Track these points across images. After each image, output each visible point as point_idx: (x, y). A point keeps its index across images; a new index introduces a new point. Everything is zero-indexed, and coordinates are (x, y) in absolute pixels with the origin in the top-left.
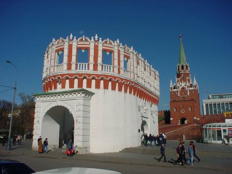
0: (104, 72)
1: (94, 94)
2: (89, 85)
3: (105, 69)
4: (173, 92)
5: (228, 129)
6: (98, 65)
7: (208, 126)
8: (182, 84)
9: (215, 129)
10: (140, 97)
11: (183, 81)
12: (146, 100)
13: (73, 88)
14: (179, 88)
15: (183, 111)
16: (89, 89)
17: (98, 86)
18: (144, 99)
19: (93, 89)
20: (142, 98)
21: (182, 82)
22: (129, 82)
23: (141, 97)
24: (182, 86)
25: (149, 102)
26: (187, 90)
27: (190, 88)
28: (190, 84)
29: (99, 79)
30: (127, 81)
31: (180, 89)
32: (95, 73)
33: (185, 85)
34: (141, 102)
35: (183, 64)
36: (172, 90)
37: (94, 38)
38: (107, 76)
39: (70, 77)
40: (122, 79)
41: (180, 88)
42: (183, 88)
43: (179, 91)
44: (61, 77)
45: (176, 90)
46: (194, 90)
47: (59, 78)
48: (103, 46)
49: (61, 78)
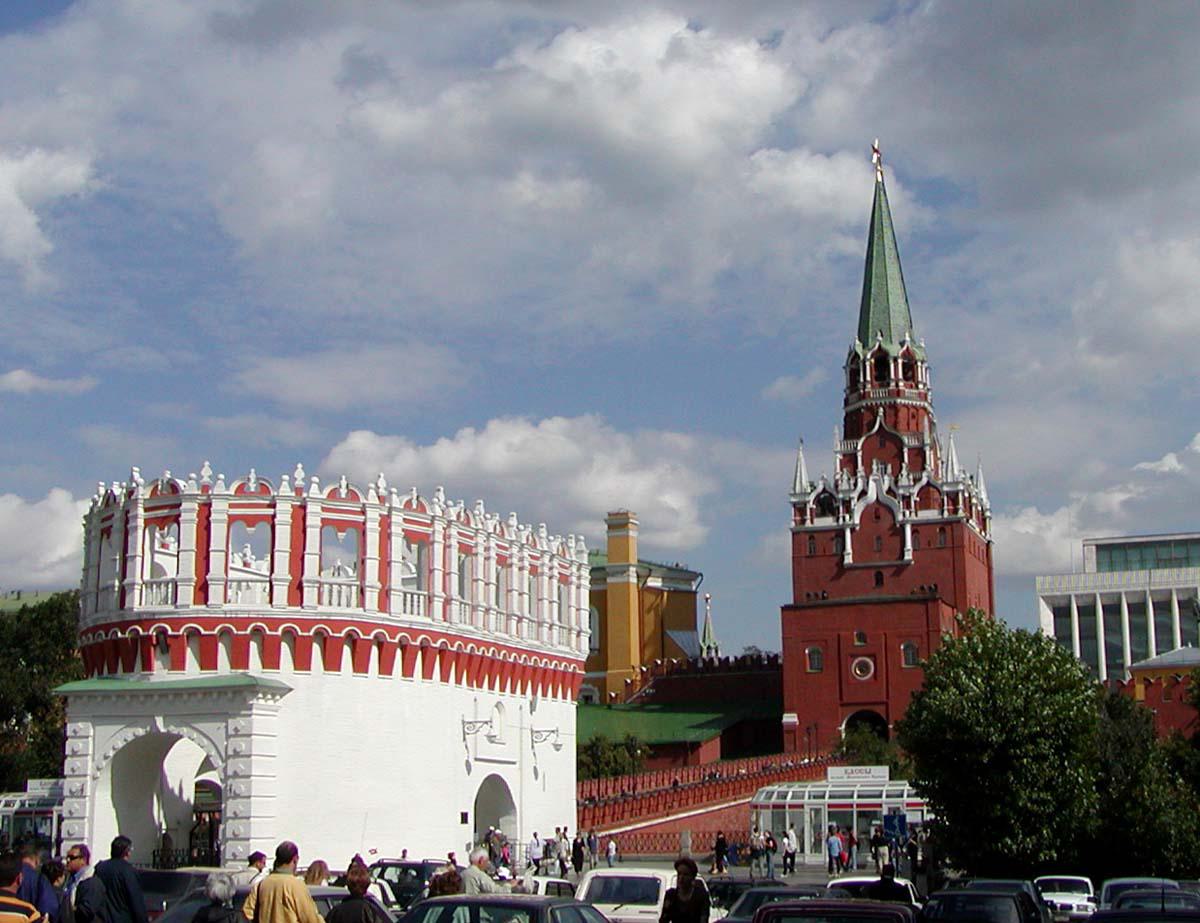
0: (324, 608)
1: (291, 690)
2: (271, 660)
3: (331, 596)
4: (813, 534)
5: (830, 806)
6: (305, 584)
7: (773, 793)
8: (872, 484)
9: (851, 806)
10: (470, 684)
11: (875, 467)
12: (503, 689)
13: (216, 668)
14: (849, 510)
15: (864, 667)
16: (270, 675)
17: (302, 662)
18: (491, 687)
19: (286, 671)
20: (480, 685)
21: (869, 471)
22: (423, 636)
23: (476, 679)
24: (872, 495)
25: (523, 692)
26: (903, 527)
27: (920, 513)
28: (924, 480)
29: (309, 636)
30: (414, 633)
31: (857, 521)
32: (295, 612)
33: (890, 491)
34: (485, 698)
35: (886, 346)
36: (803, 521)
37: (293, 479)
38: (338, 625)
39: (203, 632)
40: (393, 631)
41: (858, 508)
42: (878, 512)
43: (853, 530)
44: (173, 630)
45: (827, 522)
46: (943, 525)
47: (164, 631)
48: (324, 509)
49: (170, 632)
